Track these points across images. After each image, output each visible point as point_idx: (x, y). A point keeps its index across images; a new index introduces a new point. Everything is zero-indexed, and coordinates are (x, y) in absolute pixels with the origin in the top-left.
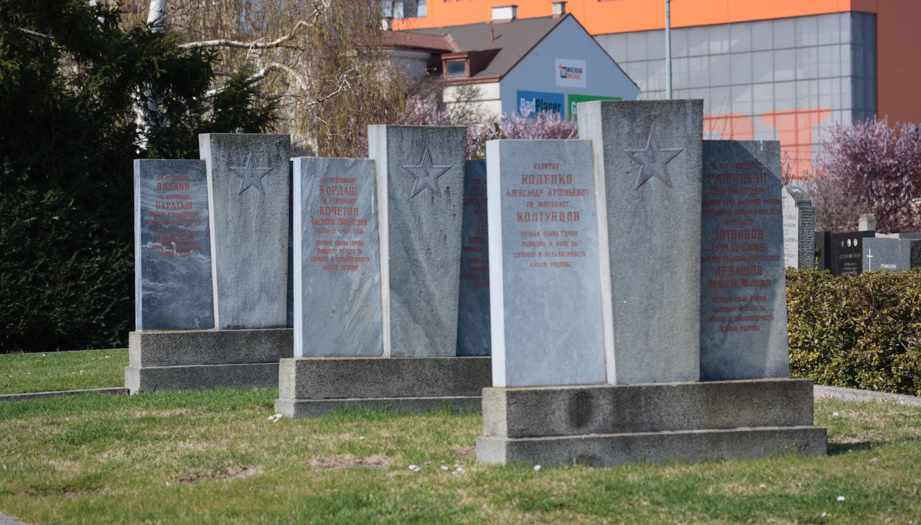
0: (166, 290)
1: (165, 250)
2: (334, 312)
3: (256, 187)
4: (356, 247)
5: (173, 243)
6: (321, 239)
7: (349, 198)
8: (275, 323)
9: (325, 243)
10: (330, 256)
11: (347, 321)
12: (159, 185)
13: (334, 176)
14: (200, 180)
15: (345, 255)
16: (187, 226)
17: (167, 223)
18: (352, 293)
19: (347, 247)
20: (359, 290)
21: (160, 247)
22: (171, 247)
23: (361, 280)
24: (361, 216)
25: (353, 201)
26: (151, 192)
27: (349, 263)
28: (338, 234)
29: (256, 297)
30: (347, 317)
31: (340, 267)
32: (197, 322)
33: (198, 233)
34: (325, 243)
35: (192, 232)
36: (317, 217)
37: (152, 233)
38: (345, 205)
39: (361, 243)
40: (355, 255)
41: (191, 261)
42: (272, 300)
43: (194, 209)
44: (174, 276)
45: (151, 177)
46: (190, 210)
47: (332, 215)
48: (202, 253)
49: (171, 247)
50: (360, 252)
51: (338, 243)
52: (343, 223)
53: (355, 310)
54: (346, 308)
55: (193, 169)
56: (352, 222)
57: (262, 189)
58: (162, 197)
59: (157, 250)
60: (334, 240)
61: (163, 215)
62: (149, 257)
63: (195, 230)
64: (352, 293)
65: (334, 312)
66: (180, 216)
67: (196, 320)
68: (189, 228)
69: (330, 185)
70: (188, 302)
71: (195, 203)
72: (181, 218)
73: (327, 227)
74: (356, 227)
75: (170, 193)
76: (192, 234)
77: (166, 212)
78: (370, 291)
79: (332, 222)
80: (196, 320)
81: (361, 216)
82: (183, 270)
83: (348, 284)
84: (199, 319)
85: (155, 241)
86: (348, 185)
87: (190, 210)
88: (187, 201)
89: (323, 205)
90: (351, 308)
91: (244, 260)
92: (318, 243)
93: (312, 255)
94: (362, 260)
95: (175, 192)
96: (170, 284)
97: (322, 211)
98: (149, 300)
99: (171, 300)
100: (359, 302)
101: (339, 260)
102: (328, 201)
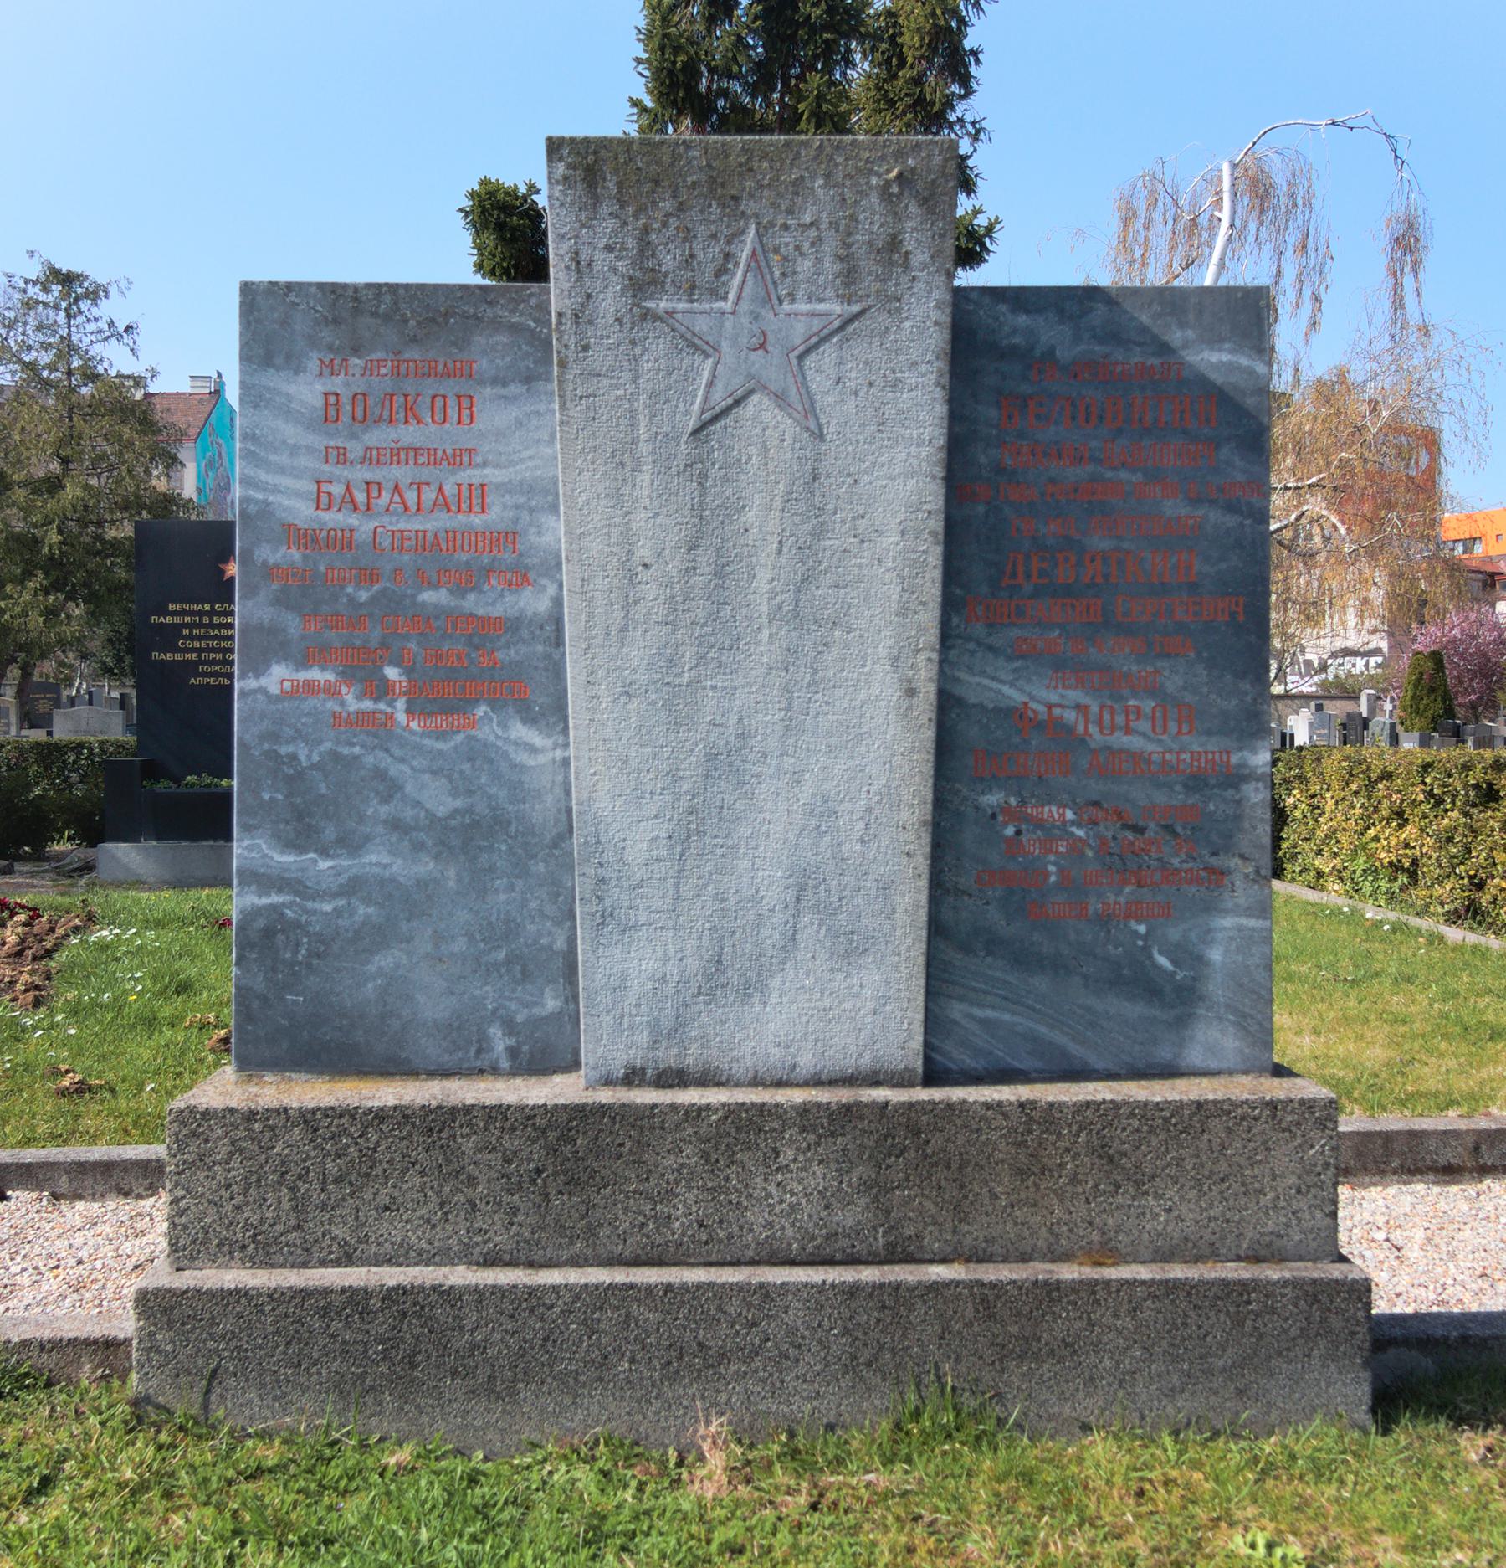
0: (353, 887)
1: (353, 701)
3: (780, 398)
5: (392, 673)
8: (866, 1062)
12: (331, 401)
14: (528, 379)
16: (460, 591)
17: (368, 576)
21: (330, 691)
22: (383, 690)
26: (291, 432)
29: (772, 936)
32: (500, 1042)
33: (512, 626)
35: (486, 622)
37: (292, 624)
41: (477, 753)
42: (851, 949)
43: (496, 515)
44: (395, 825)
45: (293, 363)
46: (477, 520)
48: (531, 720)
49: (383, 690)
55: (496, 325)
57: (810, 409)
58: (342, 457)
59: (312, 702)
61: (344, 541)
62: (275, 737)
63: (497, 611)
66: (425, 544)
67: (495, 1032)
68: (470, 603)
70: (460, 945)
71: (505, 488)
72: (436, 558)
75: (379, 436)
76: (486, 630)
77: (363, 527)
80: (495, 1032)
82: (438, 799)
84: (510, 1027)
85: (304, 662)
87: (477, 520)
88: (467, 476)
91: (711, 757)
95: (409, 434)
96: (376, 859)
98: (269, 933)
99: (378, 936)
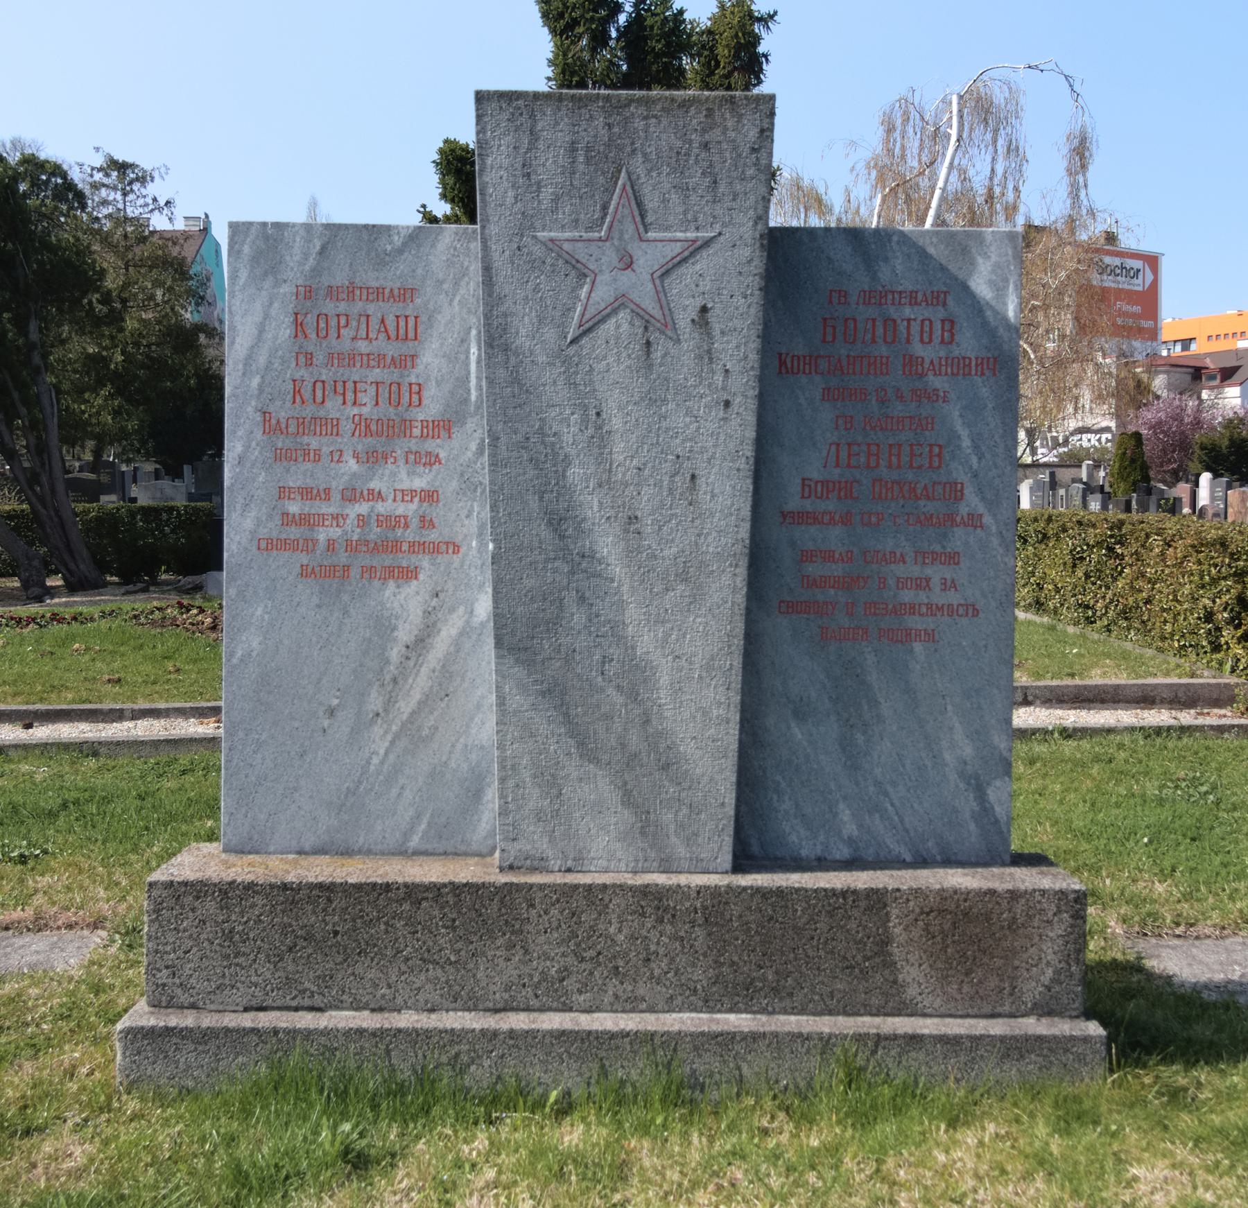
2: (331, 712)
4: (410, 509)
6: (294, 481)
7: (392, 350)
9: (307, 493)
10: (322, 535)
11: (378, 741)
13: (340, 278)
15: (375, 532)
18: (395, 654)
19: (381, 508)
20: (421, 643)
23: (427, 613)
24: (431, 408)
25: (407, 361)
27: (388, 560)
28: (352, 465)
30: (378, 730)
31: (355, 572)
34: (307, 493)
36: (283, 411)
38: (376, 374)
39: (430, 496)
40: (410, 535)
47: (333, 407)
50: (426, 523)
51: (351, 495)
52: (368, 432)
53: (405, 707)
54: (375, 701)
56: (398, 428)
60: (337, 485)
64: (395, 654)
65: (331, 712)
69: (329, 307)
73: (314, 443)
74: (413, 445)
78: (457, 644)
79: (331, 427)
81: (431, 408)
83: (384, 627)
86: (391, 310)
89: (303, 373)
90: (390, 702)
92: (284, 493)
93: (263, 532)
94: (434, 549)
97: (297, 392)
100: (420, 684)
101: (351, 547)
102: (320, 358)
